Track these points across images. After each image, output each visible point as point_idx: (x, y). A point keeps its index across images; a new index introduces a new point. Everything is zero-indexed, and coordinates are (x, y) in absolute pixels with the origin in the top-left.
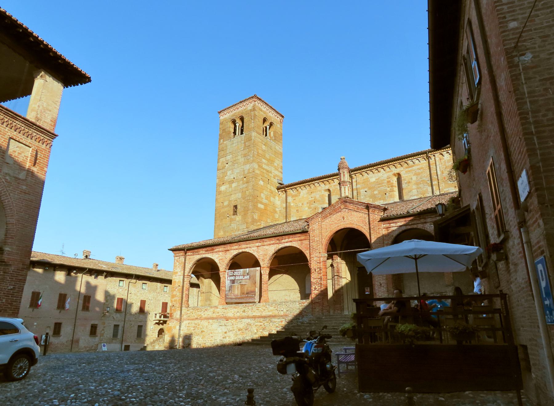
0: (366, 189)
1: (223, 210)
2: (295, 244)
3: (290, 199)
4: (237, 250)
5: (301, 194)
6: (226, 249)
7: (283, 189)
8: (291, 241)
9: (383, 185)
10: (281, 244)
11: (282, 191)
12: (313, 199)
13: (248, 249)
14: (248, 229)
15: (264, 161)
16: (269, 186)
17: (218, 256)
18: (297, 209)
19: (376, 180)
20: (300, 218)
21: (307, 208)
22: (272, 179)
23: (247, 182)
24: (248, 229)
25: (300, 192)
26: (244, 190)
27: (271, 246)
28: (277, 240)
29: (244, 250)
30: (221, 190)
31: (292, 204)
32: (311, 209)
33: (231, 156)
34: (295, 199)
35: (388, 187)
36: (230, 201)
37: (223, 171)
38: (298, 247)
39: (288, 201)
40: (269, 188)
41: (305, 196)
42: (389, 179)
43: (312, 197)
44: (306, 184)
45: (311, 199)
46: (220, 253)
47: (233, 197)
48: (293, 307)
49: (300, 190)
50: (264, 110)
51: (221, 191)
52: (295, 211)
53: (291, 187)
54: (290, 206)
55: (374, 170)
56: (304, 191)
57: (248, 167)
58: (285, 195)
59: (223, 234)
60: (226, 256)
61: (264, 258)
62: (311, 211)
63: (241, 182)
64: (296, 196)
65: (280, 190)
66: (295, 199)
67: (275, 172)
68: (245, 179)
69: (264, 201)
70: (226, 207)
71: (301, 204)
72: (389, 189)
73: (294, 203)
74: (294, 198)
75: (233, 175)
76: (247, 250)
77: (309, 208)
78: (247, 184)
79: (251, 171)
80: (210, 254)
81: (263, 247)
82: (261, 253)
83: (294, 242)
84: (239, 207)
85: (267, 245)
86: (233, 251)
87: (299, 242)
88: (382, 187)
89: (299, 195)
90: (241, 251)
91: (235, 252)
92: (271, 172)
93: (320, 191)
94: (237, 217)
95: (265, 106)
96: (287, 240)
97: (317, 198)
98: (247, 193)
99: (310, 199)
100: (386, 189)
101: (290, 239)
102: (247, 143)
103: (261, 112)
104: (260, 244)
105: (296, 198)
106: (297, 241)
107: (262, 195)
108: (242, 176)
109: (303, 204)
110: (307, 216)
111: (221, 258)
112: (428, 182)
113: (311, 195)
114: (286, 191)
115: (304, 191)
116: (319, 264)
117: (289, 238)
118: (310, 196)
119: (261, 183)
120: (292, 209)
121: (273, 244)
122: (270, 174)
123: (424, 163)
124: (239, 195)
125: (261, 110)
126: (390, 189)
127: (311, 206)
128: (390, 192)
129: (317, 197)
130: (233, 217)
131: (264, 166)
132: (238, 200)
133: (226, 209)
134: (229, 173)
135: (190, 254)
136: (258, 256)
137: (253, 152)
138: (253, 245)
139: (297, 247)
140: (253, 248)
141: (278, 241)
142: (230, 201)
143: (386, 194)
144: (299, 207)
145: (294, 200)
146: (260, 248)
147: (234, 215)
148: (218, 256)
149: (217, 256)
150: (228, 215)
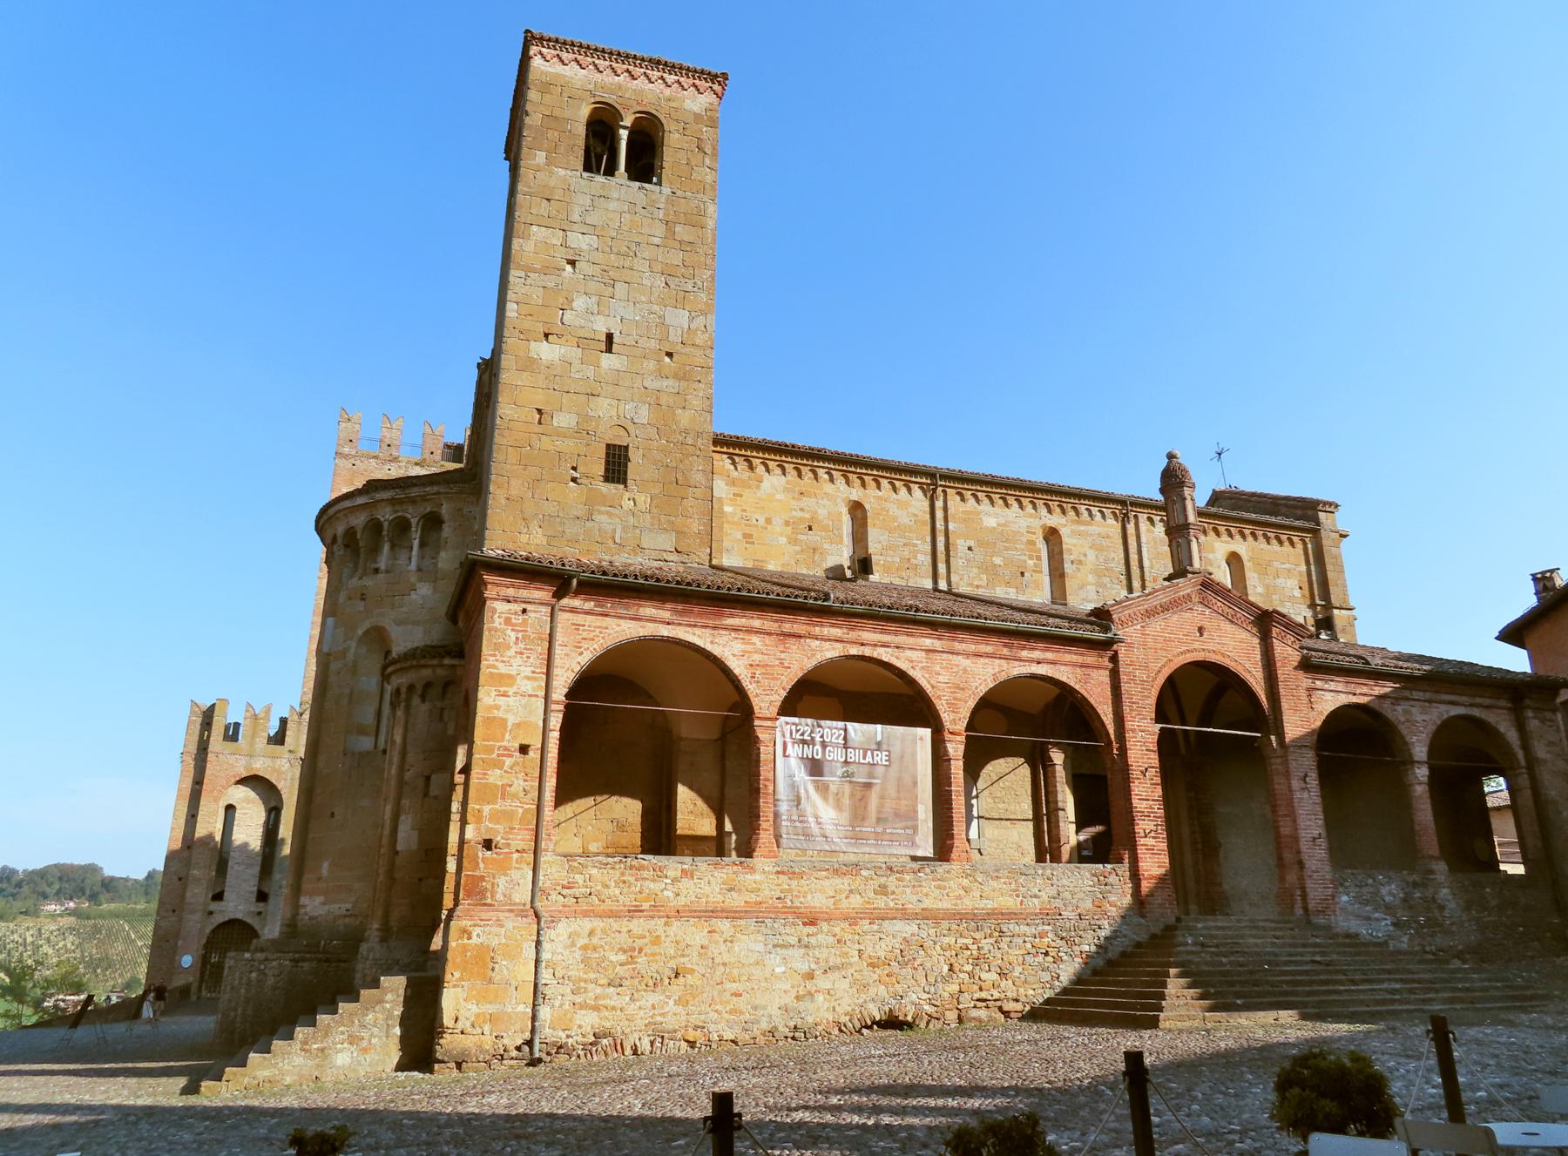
0: (971, 543)
4: (838, 645)
6: (787, 627)
8: (1053, 663)
10: (1017, 663)
12: (807, 516)
13: (890, 650)
17: (749, 648)
19: (998, 525)
27: (982, 660)
29: (867, 652)
31: (727, 509)
32: (798, 548)
34: (741, 496)
35: (1031, 558)
38: (1077, 687)
41: (778, 497)
43: (802, 510)
45: (800, 514)
46: (755, 639)
47: (604, 408)
51: (532, 361)
54: (721, 511)
55: (852, 477)
56: (774, 483)
57: (679, 319)
60: (783, 656)
61: (955, 699)
62: (797, 553)
64: (745, 485)
71: (762, 521)
73: (733, 505)
74: (736, 490)
76: (885, 655)
77: (793, 541)
81: (950, 656)
82: (941, 679)
83: (1062, 668)
85: (967, 655)
86: (818, 642)
87: (1078, 670)
89: (758, 487)
90: (854, 651)
96: (1037, 654)
100: (1026, 562)
104: (938, 644)
105: (746, 493)
106: (1074, 665)
109: (768, 521)
110: (783, 565)
111: (757, 658)
113: (798, 499)
117: (1046, 650)
118: (795, 504)
121: (988, 655)
123: (1113, 525)
126: (1035, 564)
129: (822, 513)
135: (576, 602)
136: (933, 687)
138: (911, 640)
139: (1072, 684)
140: (908, 653)
143: (1022, 574)
144: (757, 526)
145: (734, 495)
146: (938, 656)
148: (749, 648)
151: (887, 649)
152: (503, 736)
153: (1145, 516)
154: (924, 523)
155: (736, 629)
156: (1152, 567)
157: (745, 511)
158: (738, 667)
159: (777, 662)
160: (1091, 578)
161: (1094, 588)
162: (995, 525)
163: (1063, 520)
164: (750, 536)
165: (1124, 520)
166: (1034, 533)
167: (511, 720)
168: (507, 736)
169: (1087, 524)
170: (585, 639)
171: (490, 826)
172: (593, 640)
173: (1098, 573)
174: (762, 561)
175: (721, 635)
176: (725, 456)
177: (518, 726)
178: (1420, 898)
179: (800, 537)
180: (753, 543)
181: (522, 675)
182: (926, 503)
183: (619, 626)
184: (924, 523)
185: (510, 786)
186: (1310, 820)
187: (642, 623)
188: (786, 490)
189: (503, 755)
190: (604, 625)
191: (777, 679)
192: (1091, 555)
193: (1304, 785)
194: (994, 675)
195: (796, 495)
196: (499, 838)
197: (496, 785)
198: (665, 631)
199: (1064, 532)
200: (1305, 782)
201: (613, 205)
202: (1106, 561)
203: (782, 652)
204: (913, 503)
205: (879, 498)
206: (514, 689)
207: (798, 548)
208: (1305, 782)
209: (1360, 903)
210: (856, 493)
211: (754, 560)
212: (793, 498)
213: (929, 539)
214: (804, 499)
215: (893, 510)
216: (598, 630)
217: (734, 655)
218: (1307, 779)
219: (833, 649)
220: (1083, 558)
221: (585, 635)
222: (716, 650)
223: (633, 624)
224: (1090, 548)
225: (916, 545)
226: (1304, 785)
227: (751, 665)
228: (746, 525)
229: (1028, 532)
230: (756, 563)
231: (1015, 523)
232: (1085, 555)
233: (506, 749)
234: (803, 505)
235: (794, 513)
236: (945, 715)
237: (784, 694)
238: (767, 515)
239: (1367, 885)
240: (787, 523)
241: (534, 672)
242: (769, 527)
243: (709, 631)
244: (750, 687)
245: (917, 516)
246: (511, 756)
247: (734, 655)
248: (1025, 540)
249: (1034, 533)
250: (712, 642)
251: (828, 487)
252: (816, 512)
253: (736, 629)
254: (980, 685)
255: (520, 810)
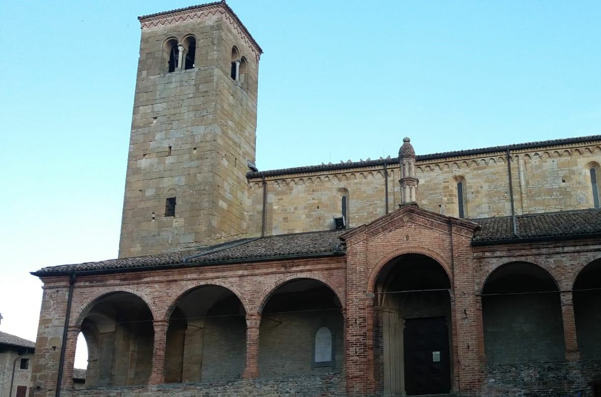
1: (142, 205)
2: (317, 276)
3: (271, 198)
4: (195, 282)
5: (295, 191)
6: (171, 278)
7: (259, 179)
8: (310, 271)
9: (437, 191)
10: (289, 274)
11: (257, 183)
12: (316, 201)
13: (221, 279)
14: (198, 244)
15: (230, 123)
16: (235, 170)
18: (285, 216)
20: (290, 232)
21: (304, 216)
22: (241, 158)
23: (200, 158)
24: (198, 244)
25: (292, 187)
26: (192, 171)
27: (270, 276)
28: (283, 266)
29: (209, 282)
30: (138, 166)
31: (275, 207)
32: (311, 219)
33: (164, 105)
34: (282, 199)
36: (158, 189)
37: (146, 130)
38: (324, 281)
39: (269, 200)
40: (236, 174)
41: (301, 195)
42: (447, 184)
43: (313, 199)
44: (305, 175)
45: (312, 201)
46: (156, 286)
47: (167, 183)
48: (309, 385)
49: (292, 184)
50: (235, 31)
51: (139, 169)
52: (281, 219)
53: (276, 178)
54: (272, 209)
56: (299, 188)
57: (201, 130)
58: (261, 191)
59: (140, 249)
60: (168, 291)
61: (253, 298)
62: (311, 222)
63: (186, 157)
64: (284, 193)
65: (253, 180)
66: (282, 199)
67: (245, 147)
68: (195, 152)
69: (229, 196)
70: (149, 199)
71: (292, 210)
72: (445, 199)
73: (278, 205)
75: (167, 140)
76: (217, 282)
77: (308, 216)
78: (200, 161)
79: (208, 139)
80: (131, 287)
81: (252, 277)
82: (246, 289)
84: (179, 202)
85: (261, 275)
86: (185, 282)
87: (326, 272)
88: (435, 195)
89: (291, 193)
90: (202, 283)
91: (191, 285)
92: (239, 146)
93: (330, 189)
94: (175, 220)
95: (236, 25)
96: (301, 268)
97: (323, 201)
98: (200, 177)
99: (309, 202)
101: (308, 267)
102: (201, 86)
103: (229, 34)
104: (246, 273)
105: (284, 197)
106: (322, 270)
107: (226, 184)
108: (188, 146)
109: (296, 209)
110: (303, 229)
111: (156, 294)
112: (506, 194)
113: (312, 194)
114: (264, 183)
115: (300, 187)
116: (362, 311)
117: (306, 265)
118: (310, 197)
119: (225, 162)
120: (274, 216)
121: (272, 273)
122: (238, 149)
124: (183, 181)
125: (230, 32)
127: (312, 213)
128: (447, 203)
129: (324, 198)
130: (165, 219)
131: (230, 133)
132: (178, 190)
133: (149, 204)
134: (158, 136)
136: (241, 294)
137: (215, 105)
138: (231, 273)
140: (230, 279)
141: (283, 269)
142: (158, 189)
144: (289, 213)
145: (279, 200)
146: (245, 278)
147: (167, 215)
148: (154, 290)
149: (148, 290)
150: (154, 216)
151: (219, 279)
152: (46, 344)
153: (523, 155)
154: (382, 191)
155: (148, 283)
156: (527, 183)
157: (284, 206)
158: (147, 299)
159: (165, 295)
160: (485, 200)
161: (487, 205)
162: (424, 183)
163: (468, 170)
164: (287, 218)
165: (509, 158)
166: (448, 182)
167: (50, 337)
168: (47, 344)
169: (484, 168)
170: (84, 298)
171: (40, 381)
172: (87, 298)
173: (489, 195)
174: (292, 230)
175: (141, 287)
176: (273, 182)
177: (52, 339)
178: (554, 377)
179: (312, 213)
180: (288, 222)
181: (55, 318)
182: (383, 180)
183: (98, 290)
184: (382, 191)
185: (47, 364)
186: (466, 336)
187: (108, 287)
188: (305, 191)
189: (46, 352)
190: (93, 291)
191: (165, 302)
192: (486, 187)
193: (465, 316)
194: (276, 282)
195: (311, 193)
196: (42, 386)
197: (42, 365)
198: (117, 289)
199: (468, 177)
200: (466, 314)
201: (173, 85)
202: (496, 188)
203: (168, 289)
204: (375, 181)
205: (356, 183)
206: (51, 325)
207: (311, 219)
208: (466, 314)
209: (503, 382)
210: (342, 185)
211: (288, 230)
212: (309, 194)
213: (384, 199)
214: (315, 193)
215: (363, 188)
216: (90, 294)
217: (146, 295)
218: (467, 312)
219: (193, 284)
220: (479, 189)
221: (85, 296)
222: (138, 294)
223: (104, 288)
224: (485, 182)
225: (376, 204)
226: (465, 316)
227: (154, 298)
228: (284, 213)
229: (444, 182)
230: (289, 231)
231: (436, 179)
232: (481, 187)
233: (47, 349)
234: (313, 196)
235: (309, 202)
236: (247, 307)
237: (167, 308)
238: (295, 206)
239: (510, 372)
240: (306, 208)
241: (59, 316)
242: (296, 212)
243: (136, 286)
244: (153, 308)
245: (377, 188)
246: (48, 352)
247: (146, 295)
248: (442, 186)
249: (448, 182)
250: (137, 290)
251: (328, 185)
252: (321, 199)
253: (148, 283)
254: (267, 289)
255: (51, 374)
